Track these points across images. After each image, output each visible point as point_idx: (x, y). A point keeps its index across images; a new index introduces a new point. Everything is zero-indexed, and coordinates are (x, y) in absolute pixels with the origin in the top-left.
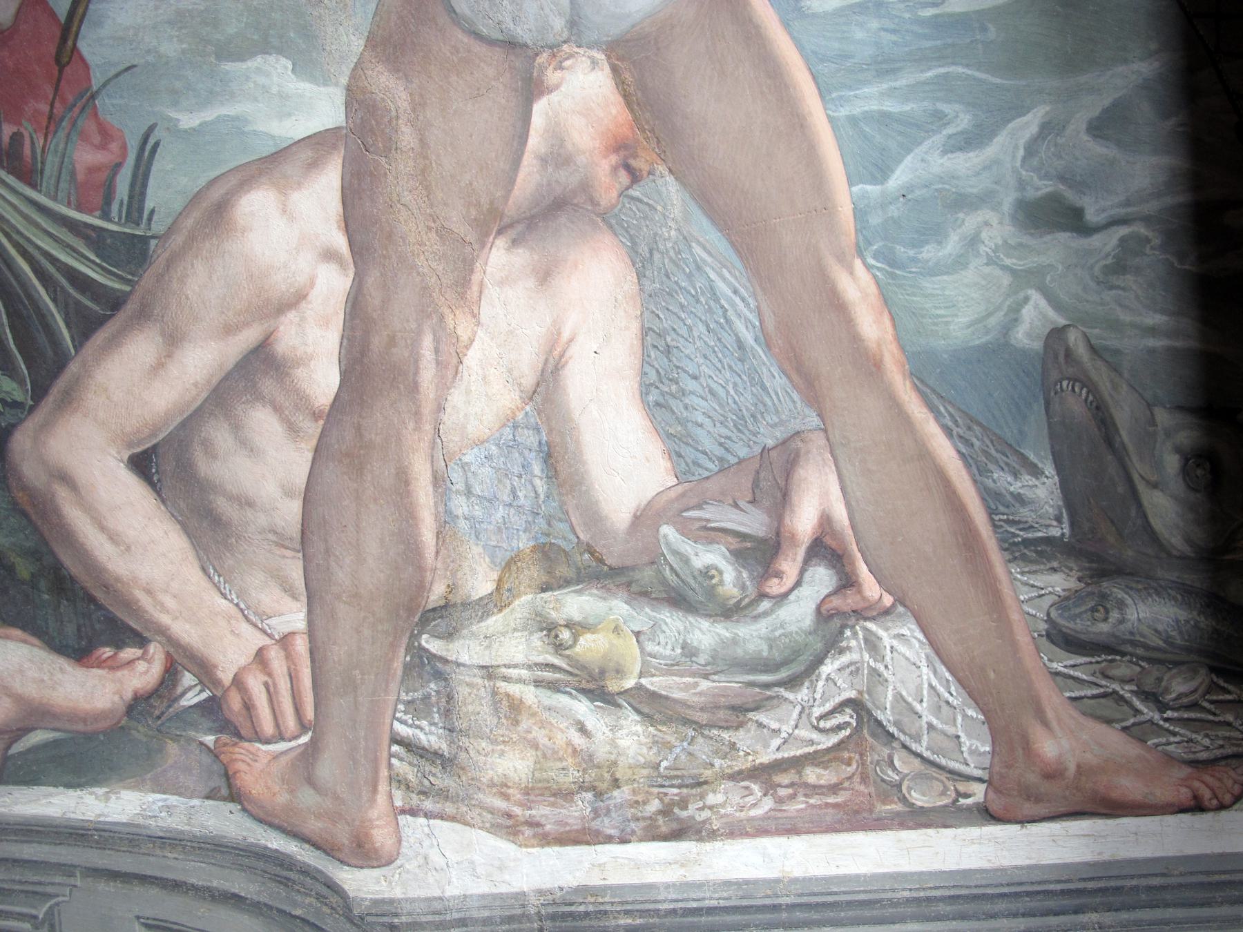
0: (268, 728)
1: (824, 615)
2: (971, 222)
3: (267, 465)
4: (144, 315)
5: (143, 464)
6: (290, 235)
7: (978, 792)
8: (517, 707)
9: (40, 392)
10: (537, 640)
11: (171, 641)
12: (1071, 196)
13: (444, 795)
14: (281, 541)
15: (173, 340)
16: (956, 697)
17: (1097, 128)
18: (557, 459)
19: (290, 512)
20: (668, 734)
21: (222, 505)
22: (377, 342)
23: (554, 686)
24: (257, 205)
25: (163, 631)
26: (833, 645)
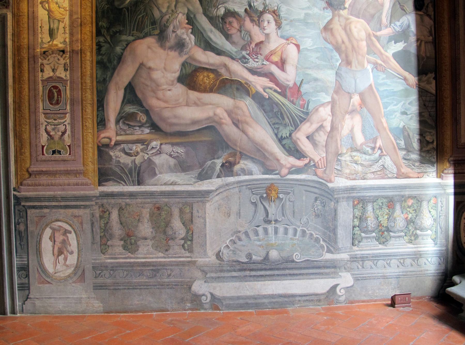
0: (321, 167)
1: (380, 155)
2: (396, 114)
3: (322, 138)
4: (308, 121)
5: (308, 138)
6: (325, 113)
7: (395, 175)
8: (348, 165)
9: (296, 129)
10: (350, 157)
11: (310, 158)
12: (406, 111)
13: (340, 174)
14: (323, 146)
15: (312, 124)
16: (393, 164)
17: (409, 104)
18: (353, 138)
19: (324, 143)
20: (364, 168)
21: (317, 142)
22: (334, 125)
23: (352, 163)
24: (321, 109)
25: (309, 156)
26: (380, 159)
